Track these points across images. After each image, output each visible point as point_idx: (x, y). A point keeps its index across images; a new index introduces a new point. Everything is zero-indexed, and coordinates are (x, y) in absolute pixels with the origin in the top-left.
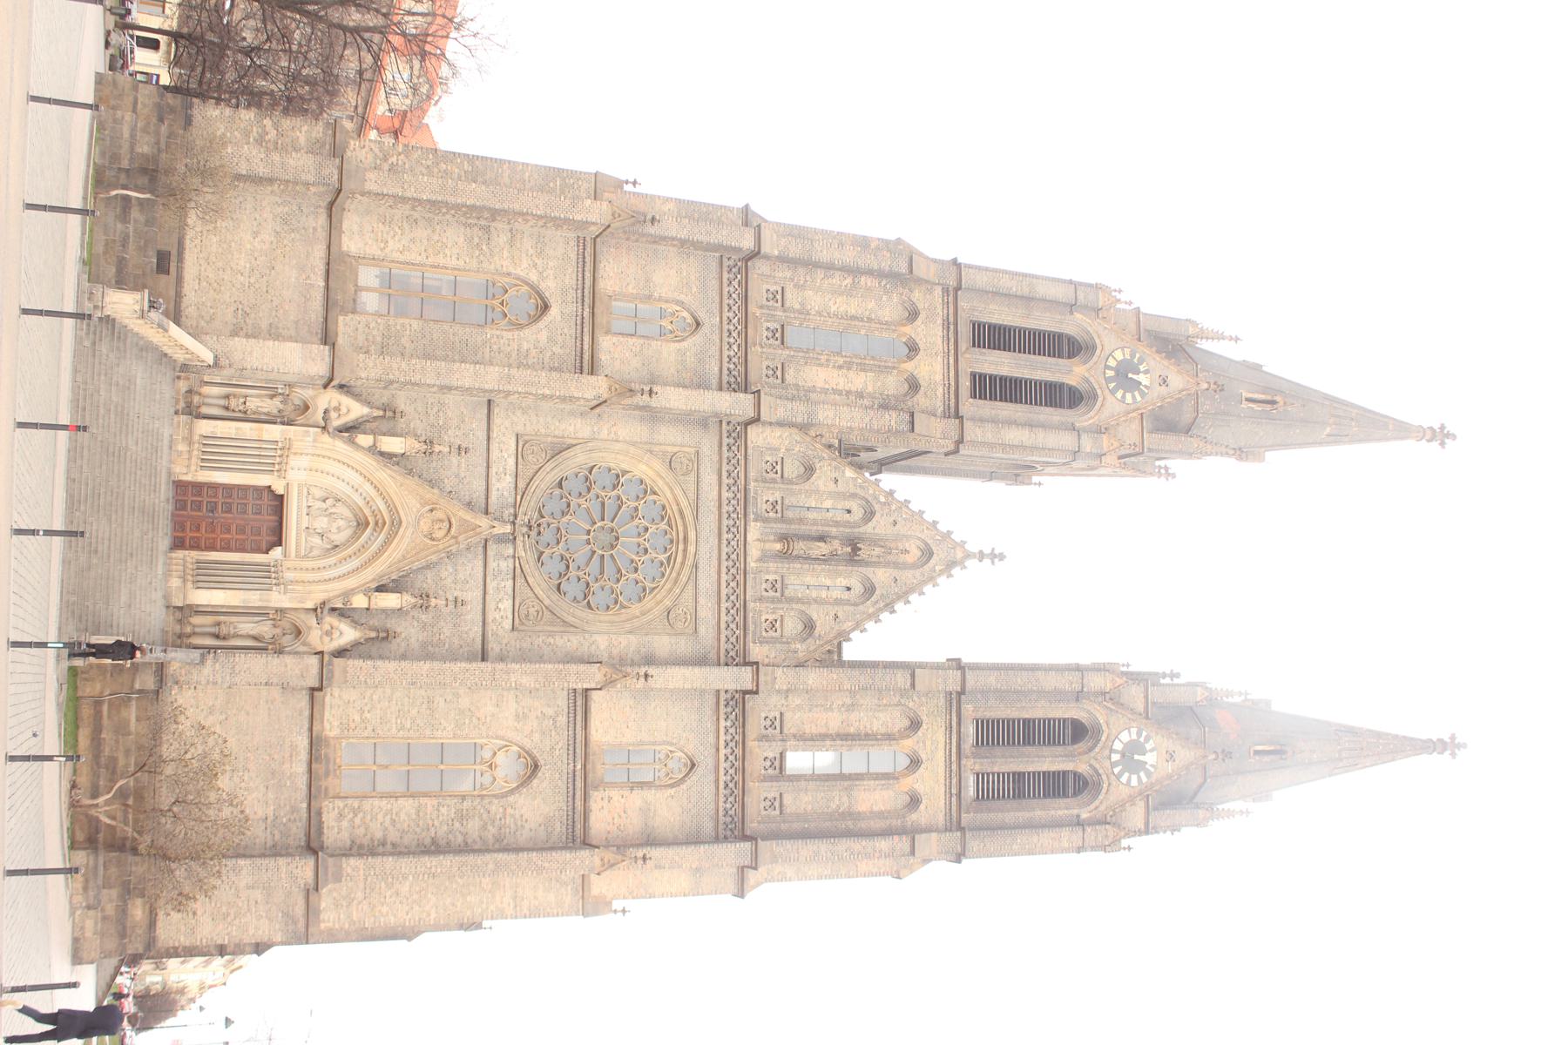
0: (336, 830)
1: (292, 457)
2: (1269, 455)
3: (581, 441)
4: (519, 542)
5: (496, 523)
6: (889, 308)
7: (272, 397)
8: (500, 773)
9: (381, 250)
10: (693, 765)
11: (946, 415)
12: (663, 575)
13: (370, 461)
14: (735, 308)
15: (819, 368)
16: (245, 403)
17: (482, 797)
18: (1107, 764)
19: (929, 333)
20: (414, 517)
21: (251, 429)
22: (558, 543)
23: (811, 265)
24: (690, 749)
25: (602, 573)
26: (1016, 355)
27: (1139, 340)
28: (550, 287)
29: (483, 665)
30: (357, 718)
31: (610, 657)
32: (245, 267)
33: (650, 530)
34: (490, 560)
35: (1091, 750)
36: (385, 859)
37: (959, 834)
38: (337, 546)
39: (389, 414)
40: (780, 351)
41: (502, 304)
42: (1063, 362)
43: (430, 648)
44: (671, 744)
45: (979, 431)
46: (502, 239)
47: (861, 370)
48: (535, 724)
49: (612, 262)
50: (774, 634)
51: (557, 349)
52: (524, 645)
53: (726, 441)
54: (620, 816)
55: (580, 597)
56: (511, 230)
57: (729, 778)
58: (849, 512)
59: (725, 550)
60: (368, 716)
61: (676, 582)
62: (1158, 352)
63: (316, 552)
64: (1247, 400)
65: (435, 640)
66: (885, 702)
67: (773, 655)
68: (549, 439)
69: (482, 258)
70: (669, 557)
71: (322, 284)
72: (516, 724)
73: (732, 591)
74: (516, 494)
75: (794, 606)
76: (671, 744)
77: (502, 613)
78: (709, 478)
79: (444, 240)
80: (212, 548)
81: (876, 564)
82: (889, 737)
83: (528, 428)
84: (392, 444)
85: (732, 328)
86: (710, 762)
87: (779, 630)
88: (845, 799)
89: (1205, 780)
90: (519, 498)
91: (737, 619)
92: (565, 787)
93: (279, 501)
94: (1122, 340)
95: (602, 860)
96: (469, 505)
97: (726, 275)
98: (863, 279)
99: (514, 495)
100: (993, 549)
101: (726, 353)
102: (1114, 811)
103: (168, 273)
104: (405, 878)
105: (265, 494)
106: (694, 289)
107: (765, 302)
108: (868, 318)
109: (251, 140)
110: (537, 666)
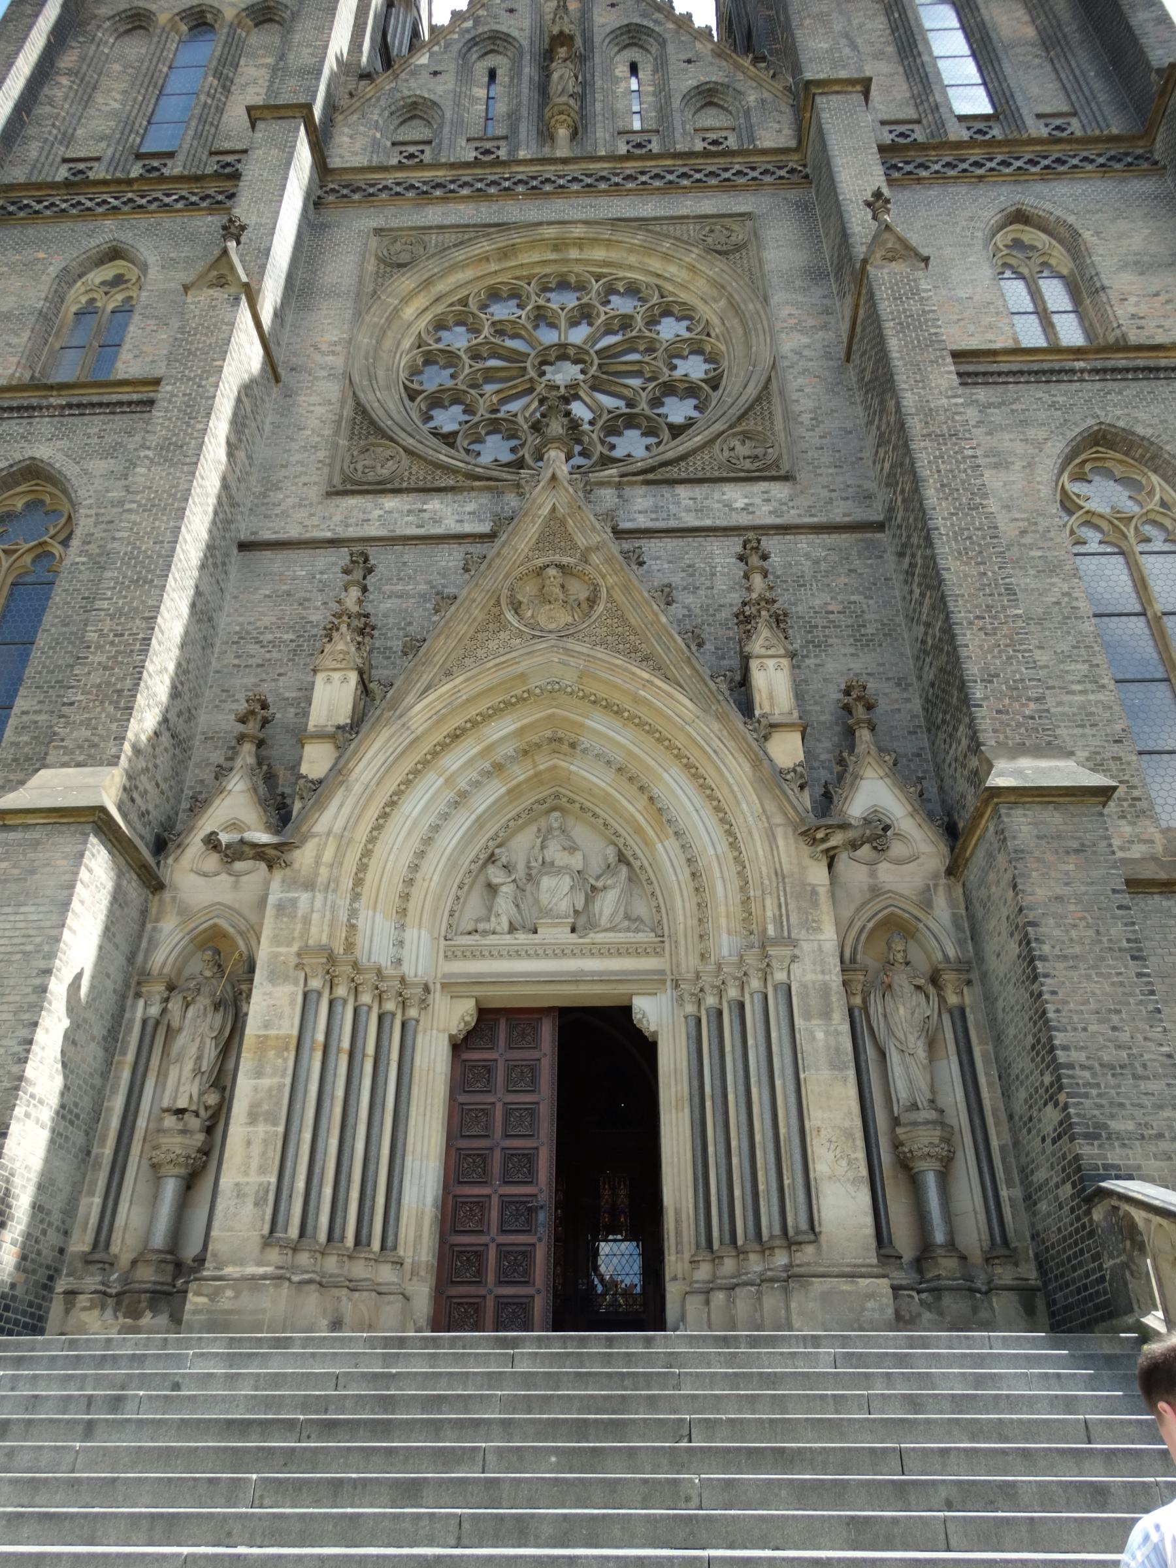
10: (1020, 217)
31: (824, 327)
33: (541, 302)
38: (622, 858)
39: (252, 727)
43: (870, 630)
48: (1007, 436)
52: (825, 460)
65: (845, 621)
67: (777, 126)
68: (343, 442)
72: (1018, 465)
77: (757, 501)
78: (433, 215)
83: (314, 479)
86: (1005, 190)
87: (724, 134)
88: (1018, 50)
90: (477, 483)
92: (1133, 384)
99: (473, 494)
105: (466, 1056)
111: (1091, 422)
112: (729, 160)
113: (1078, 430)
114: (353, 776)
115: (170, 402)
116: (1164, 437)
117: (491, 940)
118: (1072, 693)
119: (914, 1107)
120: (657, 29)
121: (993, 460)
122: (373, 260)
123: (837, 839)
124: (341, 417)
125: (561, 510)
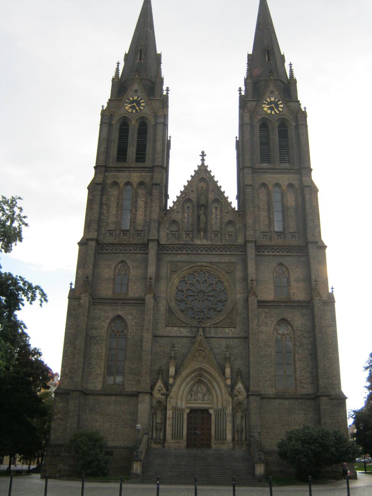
0: (308, 389)
1: (178, 406)
2: (158, 52)
3: (167, 304)
4: (204, 325)
5: (199, 334)
6: (114, 192)
7: (156, 414)
8: (286, 332)
9: (100, 375)
11: (153, 172)
12: (214, 274)
13: (178, 379)
14: (116, 248)
15: (137, 218)
16: (159, 423)
17: (294, 338)
18: (276, 115)
19: (122, 178)
20: (198, 363)
21: (169, 421)
22: (203, 312)
23: (100, 221)
24: (275, 265)
25: (214, 296)
26: (128, 146)
27: (121, 100)
28: (111, 315)
29: (250, 338)
30: (268, 382)
32: (109, 424)
33: (198, 279)
34: (211, 336)
35: (271, 122)
36: (319, 372)
37: (302, 170)
38: (208, 390)
39: (160, 372)
40: (132, 232)
41: (118, 332)
42: (130, 129)
44: (274, 272)
45: (158, 160)
46: (95, 332)
47: (137, 203)
49: (101, 293)
50: (233, 235)
51: (134, 312)
53: (165, 252)
54: (300, 290)
55: (222, 304)
56: (91, 329)
57: (285, 251)
58: (188, 207)
59: (204, 252)
60: (268, 378)
61: (216, 270)
62: (125, 93)
63: (210, 397)
64: (140, 60)
66: (256, 196)
67: (241, 235)
68: (167, 315)
69: (102, 339)
70: (208, 272)
71: (114, 397)
73: (219, 250)
74: (187, 327)
75: (223, 227)
76: (274, 272)
77: (230, 331)
78: (179, 258)
79: (96, 353)
80: (210, 434)
81: (207, 198)
82: (269, 194)
84: (172, 371)
85: (124, 249)
88: (291, 210)
89: (280, 80)
90: (188, 326)
91: (229, 248)
93: (193, 411)
94: (121, 106)
95: (317, 296)
96: (193, 343)
97: (105, 251)
98: (103, 201)
100: (200, 155)
101: (133, 251)
102: (292, 114)
103: (112, 452)
104: (325, 365)
106: (110, 263)
107: (113, 237)
108: (118, 200)
109: (62, 423)
110: (250, 319)
111: (282, 317)
112: (232, 246)
113: (279, 319)
114: (176, 383)
115: (146, 320)
116: (292, 321)
117: (192, 402)
118: (268, 368)
119: (239, 425)
120: (221, 201)
121: (266, 325)
122: (169, 270)
123: (233, 396)
124: (166, 310)
125: (202, 340)
